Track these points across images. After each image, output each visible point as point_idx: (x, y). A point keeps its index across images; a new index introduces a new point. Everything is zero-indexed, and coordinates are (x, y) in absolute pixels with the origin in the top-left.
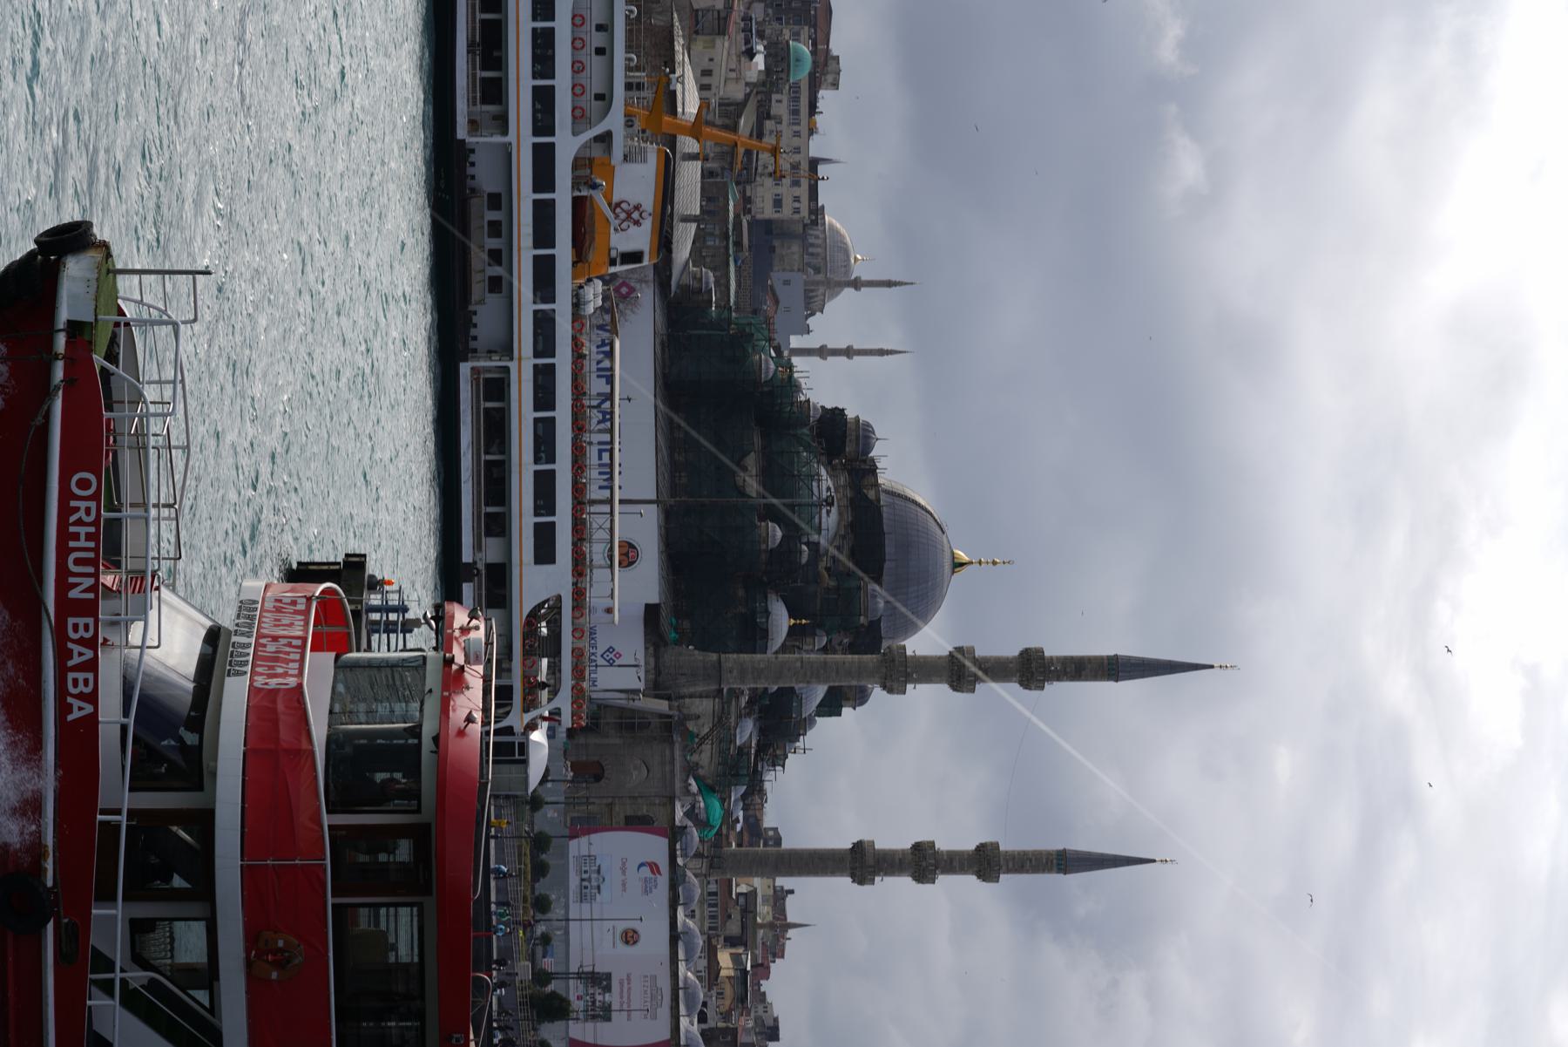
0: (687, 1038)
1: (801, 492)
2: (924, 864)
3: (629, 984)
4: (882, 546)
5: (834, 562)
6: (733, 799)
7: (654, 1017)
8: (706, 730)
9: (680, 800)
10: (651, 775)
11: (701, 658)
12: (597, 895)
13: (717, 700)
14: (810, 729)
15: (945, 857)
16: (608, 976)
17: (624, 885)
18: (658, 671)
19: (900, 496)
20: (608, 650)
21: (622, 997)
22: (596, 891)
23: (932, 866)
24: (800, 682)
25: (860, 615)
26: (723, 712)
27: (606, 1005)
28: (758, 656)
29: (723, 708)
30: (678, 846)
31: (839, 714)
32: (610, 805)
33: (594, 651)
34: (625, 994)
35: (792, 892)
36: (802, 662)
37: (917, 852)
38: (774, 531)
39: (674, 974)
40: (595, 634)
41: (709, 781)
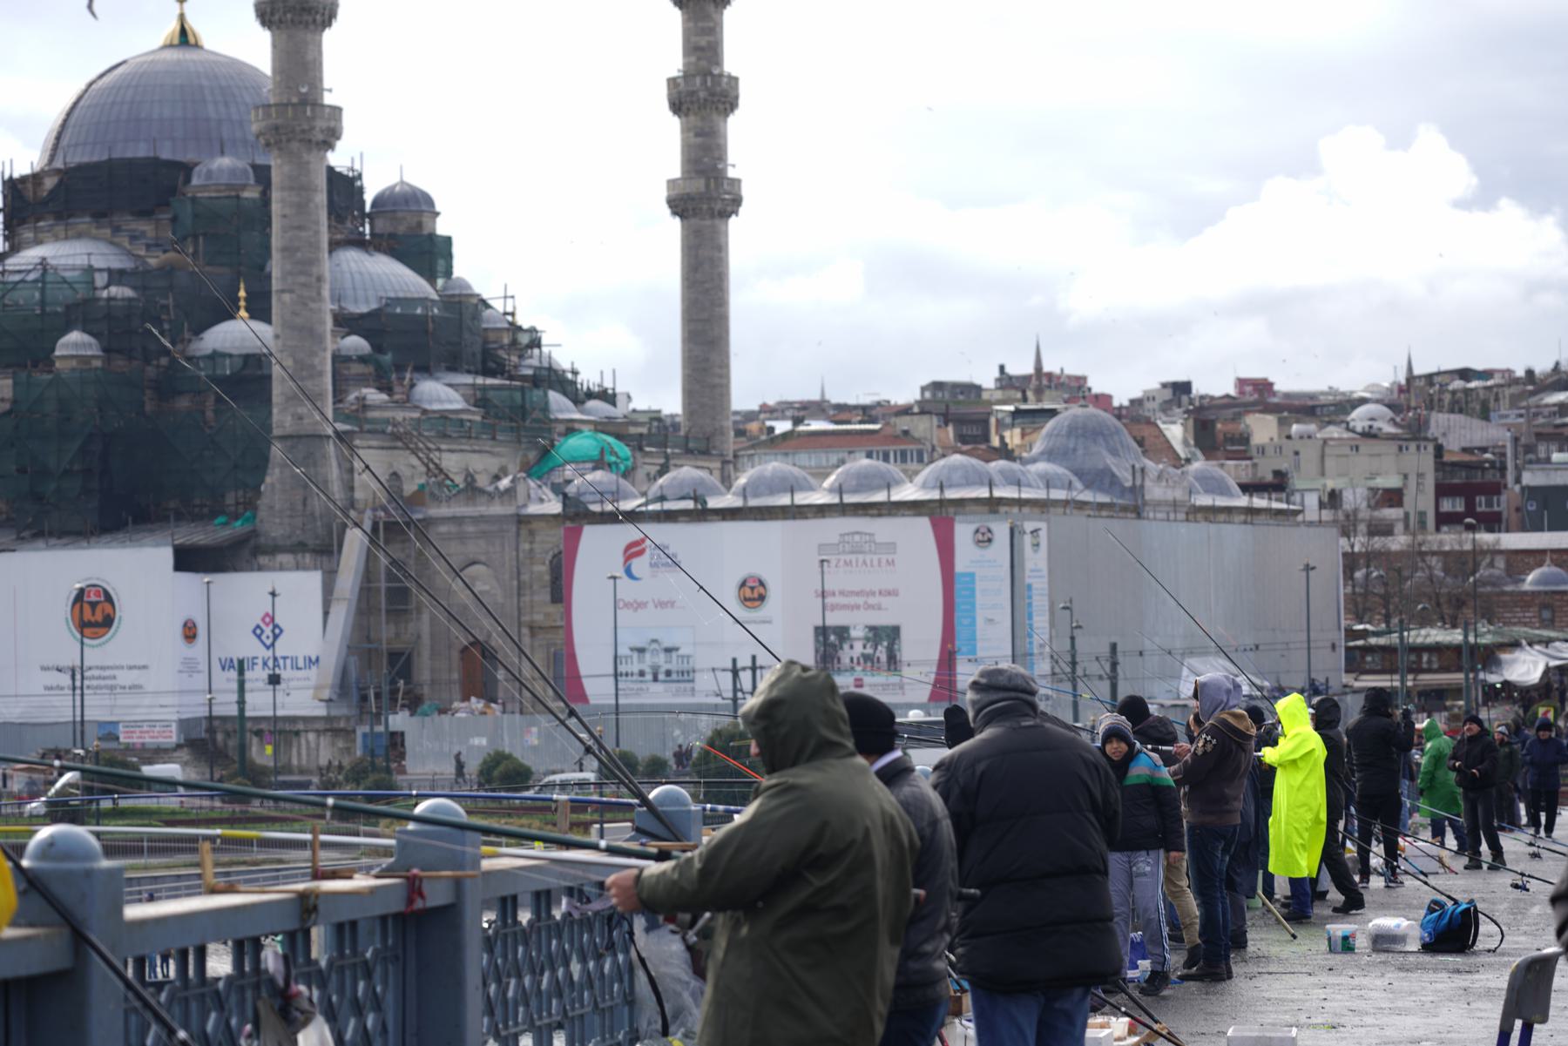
0: (933, 488)
1: (21, 302)
2: (702, 95)
3: (873, 594)
4: (131, 163)
5: (157, 245)
6: (577, 416)
7: (891, 547)
8: (415, 461)
9: (525, 506)
10: (483, 558)
11: (277, 471)
12: (681, 652)
13: (357, 442)
14: (468, 287)
15: (693, 59)
16: (822, 632)
17: (662, 605)
18: (298, 548)
19: (58, 138)
20: (259, 637)
21: (857, 607)
22: (674, 655)
23: (706, 82)
24: (319, 294)
25: (238, 197)
26: (383, 432)
27: (871, 635)
28: (276, 370)
29: (369, 432)
30: (596, 508)
31: (448, 241)
32: (534, 629)
33: (260, 661)
34: (853, 600)
35: (1002, 368)
36: (283, 291)
37: (684, 107)
38: (66, 346)
39: (821, 511)
40: (232, 661)
41: (532, 455)
